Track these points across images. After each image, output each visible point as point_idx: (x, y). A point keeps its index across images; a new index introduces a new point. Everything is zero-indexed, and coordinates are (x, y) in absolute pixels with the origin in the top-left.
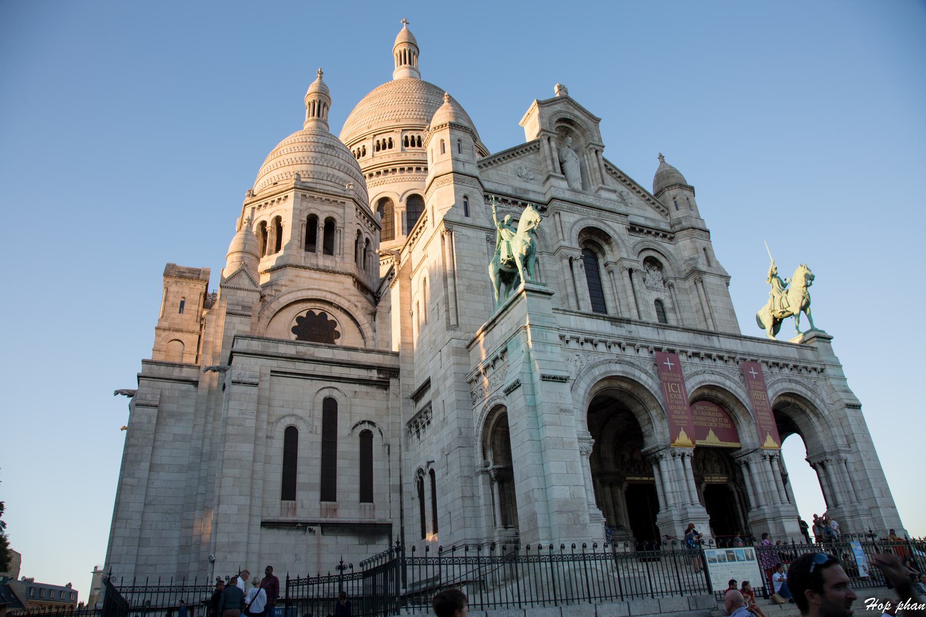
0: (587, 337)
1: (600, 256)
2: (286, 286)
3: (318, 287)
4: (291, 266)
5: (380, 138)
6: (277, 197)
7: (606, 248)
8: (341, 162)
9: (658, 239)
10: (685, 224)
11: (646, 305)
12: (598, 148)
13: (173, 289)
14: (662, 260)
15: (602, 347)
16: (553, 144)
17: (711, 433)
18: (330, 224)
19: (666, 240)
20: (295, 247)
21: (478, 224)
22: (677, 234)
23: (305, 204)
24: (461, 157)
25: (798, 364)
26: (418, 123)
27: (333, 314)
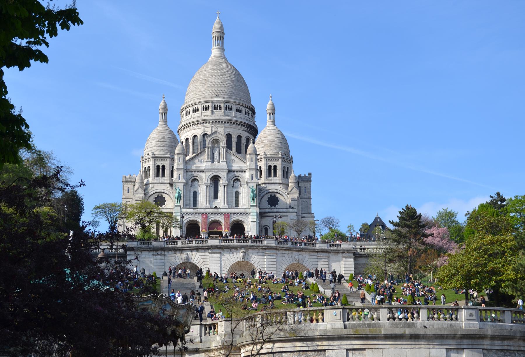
2: (152, 189)
5: (194, 107)
6: (148, 160)
7: (220, 180)
8: (167, 143)
11: (232, 193)
14: (240, 179)
16: (209, 149)
17: (215, 229)
18: (163, 167)
20: (153, 177)
21: (182, 182)
22: (246, 170)
23: (157, 162)
26: (207, 99)
27: (164, 195)
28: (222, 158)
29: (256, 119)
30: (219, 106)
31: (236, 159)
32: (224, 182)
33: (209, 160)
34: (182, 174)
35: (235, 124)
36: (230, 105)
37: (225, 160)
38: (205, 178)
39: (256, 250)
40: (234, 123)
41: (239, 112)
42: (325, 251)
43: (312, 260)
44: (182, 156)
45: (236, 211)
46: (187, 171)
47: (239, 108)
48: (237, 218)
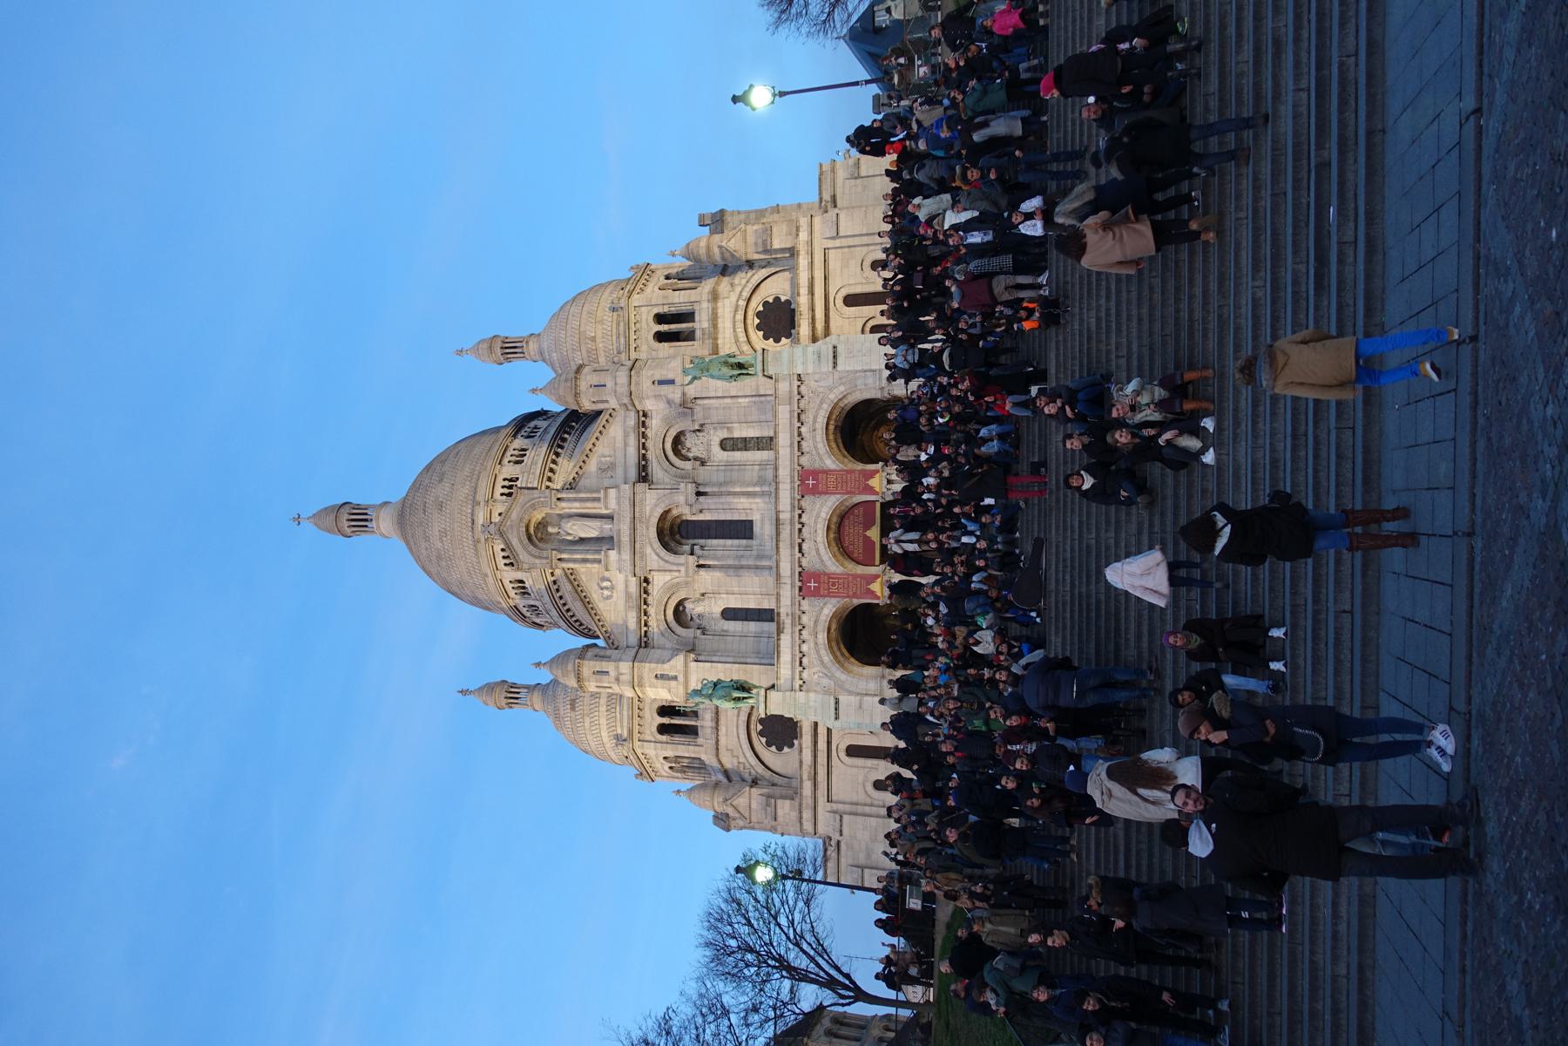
0: (798, 663)
1: (684, 518)
2: (738, 757)
3: (735, 729)
4: (717, 755)
5: (512, 593)
7: (675, 512)
9: (649, 433)
10: (626, 400)
11: (729, 465)
12: (554, 500)
15: (805, 648)
17: (868, 533)
19: (648, 422)
24: (613, 674)
25: (796, 415)
28: (596, 504)
31: (599, 449)
32: (681, 499)
33: (601, 556)
34: (653, 665)
35: (553, 466)
36: (500, 483)
37: (601, 495)
40: (552, 470)
45: (788, 442)
48: (820, 435)
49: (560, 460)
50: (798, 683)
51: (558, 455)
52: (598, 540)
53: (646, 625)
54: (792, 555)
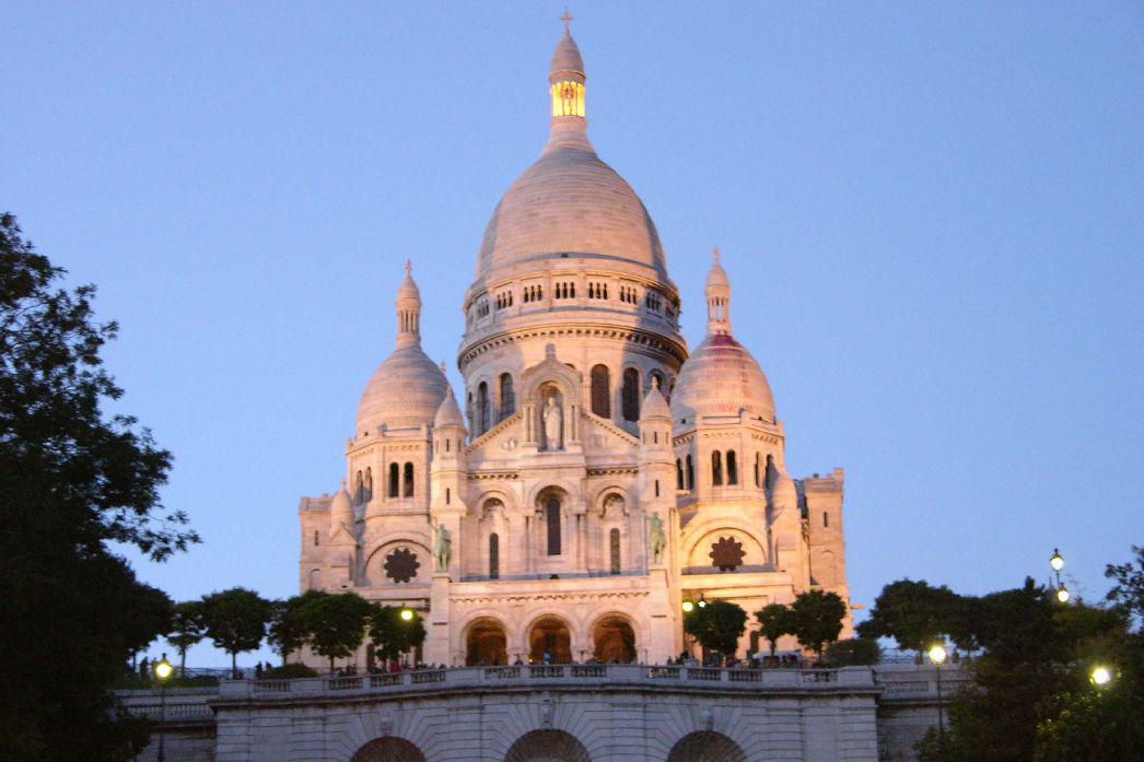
1: (562, 504)
5: (499, 292)
7: (565, 498)
13: (309, 524)
15: (477, 602)
18: (409, 467)
24: (448, 454)
29: (682, 320)
30: (569, 287)
33: (533, 443)
35: (618, 335)
36: (602, 281)
37: (577, 441)
38: (520, 495)
39: (586, 698)
40: (614, 334)
41: (629, 301)
42: (791, 693)
43: (752, 719)
44: (454, 432)
46: (471, 477)
47: (629, 289)
49: (624, 341)
50: (454, 598)
51: (629, 338)
52: (544, 437)
53: (485, 477)
54: (535, 592)
